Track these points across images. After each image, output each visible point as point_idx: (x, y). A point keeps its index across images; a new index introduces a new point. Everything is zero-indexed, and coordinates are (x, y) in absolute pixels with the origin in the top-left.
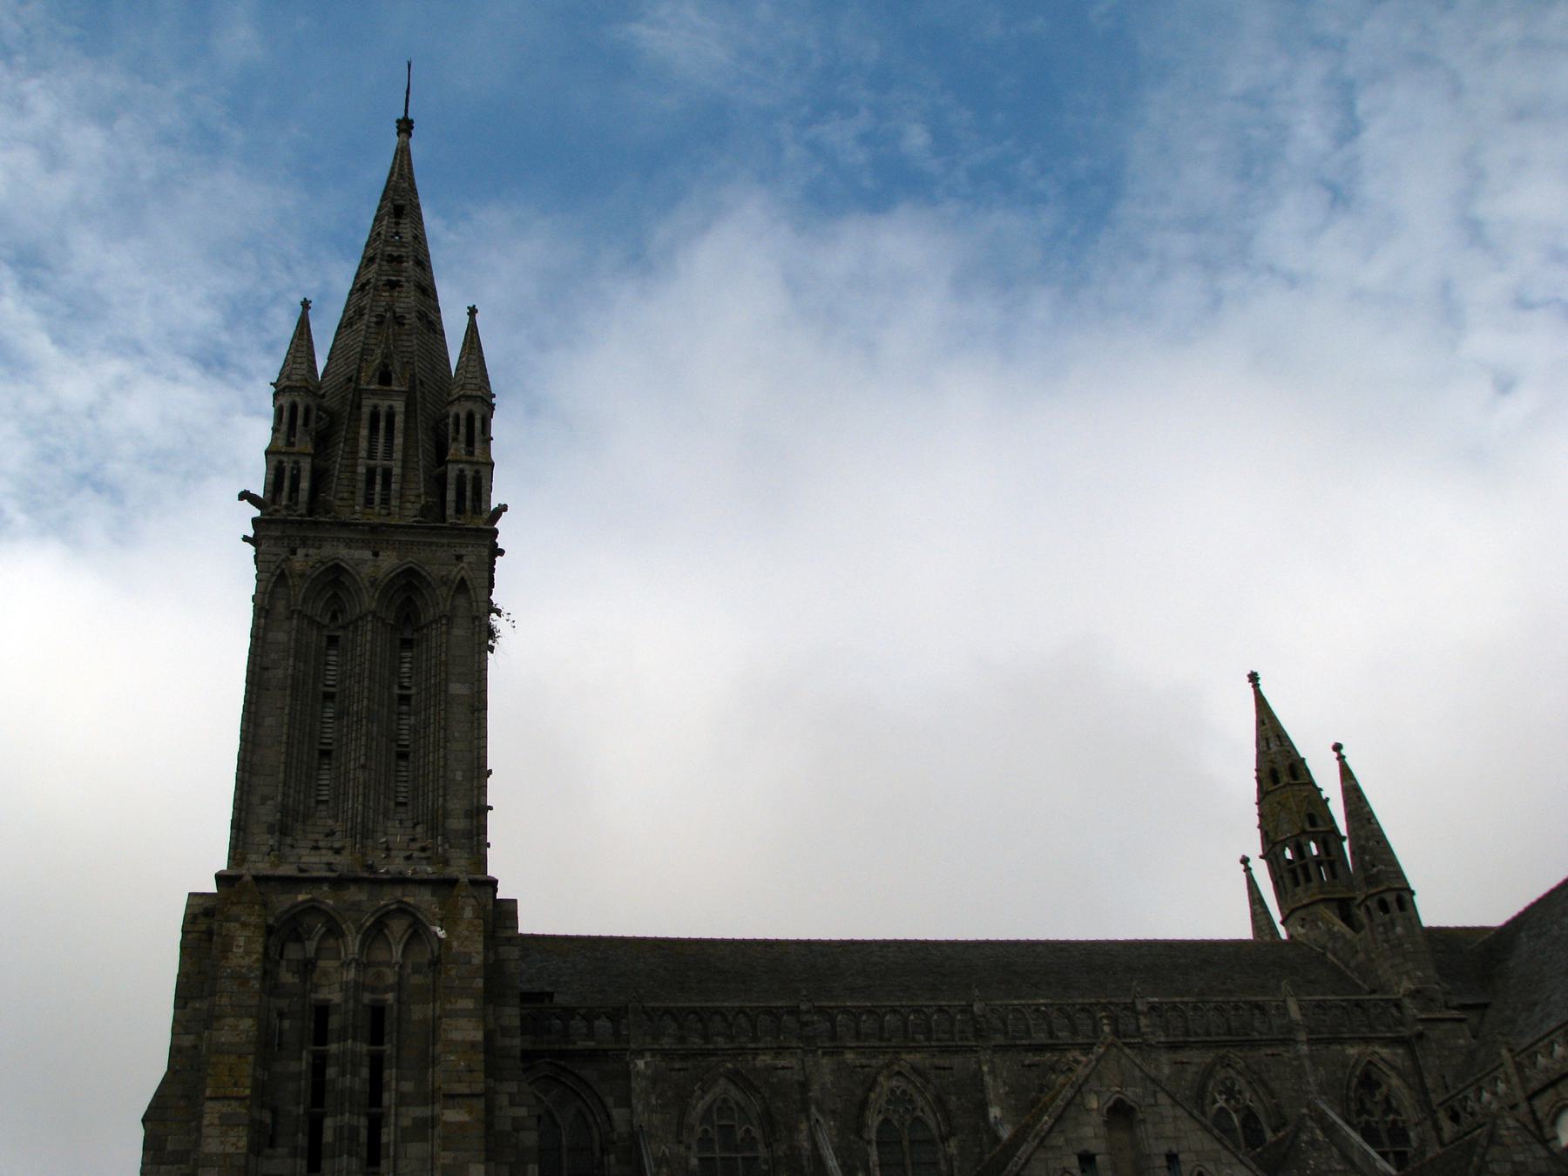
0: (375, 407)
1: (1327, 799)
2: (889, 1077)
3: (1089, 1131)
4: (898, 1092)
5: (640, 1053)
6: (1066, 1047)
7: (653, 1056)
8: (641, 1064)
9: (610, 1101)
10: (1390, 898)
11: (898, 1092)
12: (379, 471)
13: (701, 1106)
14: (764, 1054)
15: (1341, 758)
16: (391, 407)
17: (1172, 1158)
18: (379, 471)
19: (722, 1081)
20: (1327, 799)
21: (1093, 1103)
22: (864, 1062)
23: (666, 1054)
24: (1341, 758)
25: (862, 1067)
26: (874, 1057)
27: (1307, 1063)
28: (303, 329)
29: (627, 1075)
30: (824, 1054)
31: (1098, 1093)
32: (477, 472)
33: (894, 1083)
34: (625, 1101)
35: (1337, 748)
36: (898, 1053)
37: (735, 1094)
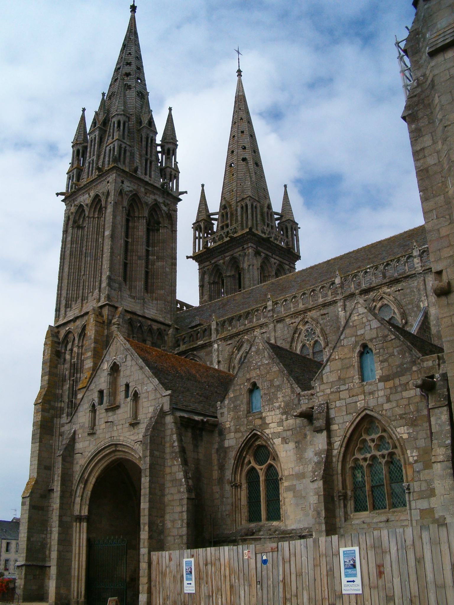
4: (310, 330)
6: (378, 287)
7: (221, 341)
11: (310, 330)
13: (238, 357)
14: (256, 329)
17: (127, 386)
25: (292, 323)
26: (297, 317)
28: (83, 118)
33: (307, 327)
36: (305, 313)
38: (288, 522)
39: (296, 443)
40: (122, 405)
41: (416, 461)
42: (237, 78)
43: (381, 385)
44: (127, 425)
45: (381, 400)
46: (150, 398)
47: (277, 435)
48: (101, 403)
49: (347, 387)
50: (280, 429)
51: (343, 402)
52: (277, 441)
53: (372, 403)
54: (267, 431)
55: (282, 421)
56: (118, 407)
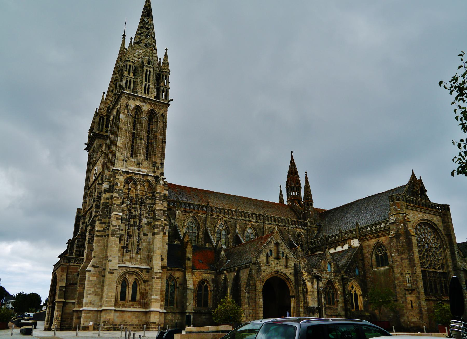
0: (147, 69)
1: (300, 180)
2: (220, 221)
3: (272, 246)
5: (178, 210)
8: (178, 212)
9: (171, 218)
10: (310, 203)
12: (147, 85)
15: (306, 175)
16: (150, 70)
17: (283, 252)
18: (147, 85)
19: (191, 218)
20: (300, 180)
21: (273, 242)
22: (216, 218)
23: (182, 211)
24: (306, 175)
25: (216, 219)
27: (290, 231)
29: (175, 214)
30: (210, 215)
31: (274, 240)
32: (167, 90)
34: (174, 219)
35: (306, 172)
37: (193, 220)
38: (309, 304)
39: (312, 282)
40: (281, 259)
41: (340, 295)
42: (122, 39)
43: (333, 274)
44: (284, 266)
45: (333, 277)
46: (293, 260)
47: (307, 279)
48: (271, 254)
49: (325, 271)
50: (307, 277)
51: (324, 275)
52: (306, 281)
53: (331, 277)
54: (303, 277)
55: (308, 275)
56: (280, 259)
